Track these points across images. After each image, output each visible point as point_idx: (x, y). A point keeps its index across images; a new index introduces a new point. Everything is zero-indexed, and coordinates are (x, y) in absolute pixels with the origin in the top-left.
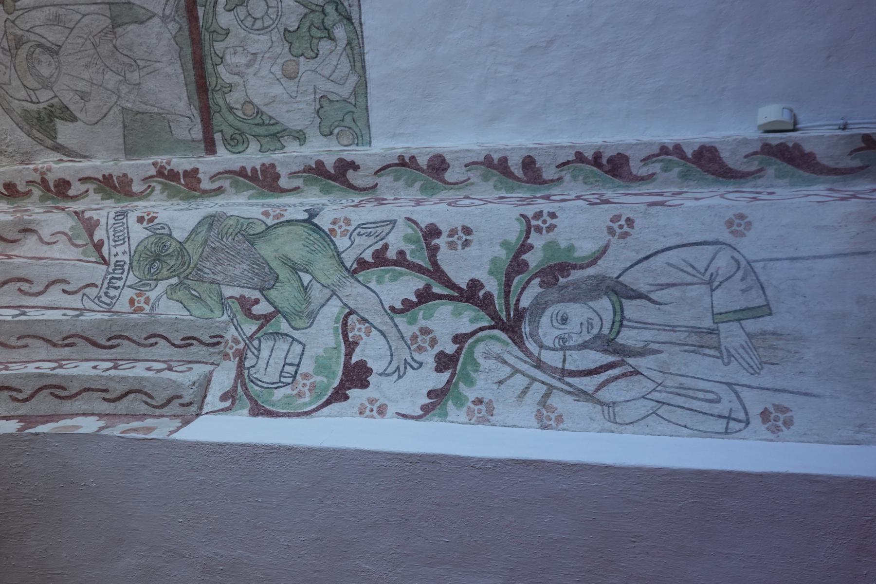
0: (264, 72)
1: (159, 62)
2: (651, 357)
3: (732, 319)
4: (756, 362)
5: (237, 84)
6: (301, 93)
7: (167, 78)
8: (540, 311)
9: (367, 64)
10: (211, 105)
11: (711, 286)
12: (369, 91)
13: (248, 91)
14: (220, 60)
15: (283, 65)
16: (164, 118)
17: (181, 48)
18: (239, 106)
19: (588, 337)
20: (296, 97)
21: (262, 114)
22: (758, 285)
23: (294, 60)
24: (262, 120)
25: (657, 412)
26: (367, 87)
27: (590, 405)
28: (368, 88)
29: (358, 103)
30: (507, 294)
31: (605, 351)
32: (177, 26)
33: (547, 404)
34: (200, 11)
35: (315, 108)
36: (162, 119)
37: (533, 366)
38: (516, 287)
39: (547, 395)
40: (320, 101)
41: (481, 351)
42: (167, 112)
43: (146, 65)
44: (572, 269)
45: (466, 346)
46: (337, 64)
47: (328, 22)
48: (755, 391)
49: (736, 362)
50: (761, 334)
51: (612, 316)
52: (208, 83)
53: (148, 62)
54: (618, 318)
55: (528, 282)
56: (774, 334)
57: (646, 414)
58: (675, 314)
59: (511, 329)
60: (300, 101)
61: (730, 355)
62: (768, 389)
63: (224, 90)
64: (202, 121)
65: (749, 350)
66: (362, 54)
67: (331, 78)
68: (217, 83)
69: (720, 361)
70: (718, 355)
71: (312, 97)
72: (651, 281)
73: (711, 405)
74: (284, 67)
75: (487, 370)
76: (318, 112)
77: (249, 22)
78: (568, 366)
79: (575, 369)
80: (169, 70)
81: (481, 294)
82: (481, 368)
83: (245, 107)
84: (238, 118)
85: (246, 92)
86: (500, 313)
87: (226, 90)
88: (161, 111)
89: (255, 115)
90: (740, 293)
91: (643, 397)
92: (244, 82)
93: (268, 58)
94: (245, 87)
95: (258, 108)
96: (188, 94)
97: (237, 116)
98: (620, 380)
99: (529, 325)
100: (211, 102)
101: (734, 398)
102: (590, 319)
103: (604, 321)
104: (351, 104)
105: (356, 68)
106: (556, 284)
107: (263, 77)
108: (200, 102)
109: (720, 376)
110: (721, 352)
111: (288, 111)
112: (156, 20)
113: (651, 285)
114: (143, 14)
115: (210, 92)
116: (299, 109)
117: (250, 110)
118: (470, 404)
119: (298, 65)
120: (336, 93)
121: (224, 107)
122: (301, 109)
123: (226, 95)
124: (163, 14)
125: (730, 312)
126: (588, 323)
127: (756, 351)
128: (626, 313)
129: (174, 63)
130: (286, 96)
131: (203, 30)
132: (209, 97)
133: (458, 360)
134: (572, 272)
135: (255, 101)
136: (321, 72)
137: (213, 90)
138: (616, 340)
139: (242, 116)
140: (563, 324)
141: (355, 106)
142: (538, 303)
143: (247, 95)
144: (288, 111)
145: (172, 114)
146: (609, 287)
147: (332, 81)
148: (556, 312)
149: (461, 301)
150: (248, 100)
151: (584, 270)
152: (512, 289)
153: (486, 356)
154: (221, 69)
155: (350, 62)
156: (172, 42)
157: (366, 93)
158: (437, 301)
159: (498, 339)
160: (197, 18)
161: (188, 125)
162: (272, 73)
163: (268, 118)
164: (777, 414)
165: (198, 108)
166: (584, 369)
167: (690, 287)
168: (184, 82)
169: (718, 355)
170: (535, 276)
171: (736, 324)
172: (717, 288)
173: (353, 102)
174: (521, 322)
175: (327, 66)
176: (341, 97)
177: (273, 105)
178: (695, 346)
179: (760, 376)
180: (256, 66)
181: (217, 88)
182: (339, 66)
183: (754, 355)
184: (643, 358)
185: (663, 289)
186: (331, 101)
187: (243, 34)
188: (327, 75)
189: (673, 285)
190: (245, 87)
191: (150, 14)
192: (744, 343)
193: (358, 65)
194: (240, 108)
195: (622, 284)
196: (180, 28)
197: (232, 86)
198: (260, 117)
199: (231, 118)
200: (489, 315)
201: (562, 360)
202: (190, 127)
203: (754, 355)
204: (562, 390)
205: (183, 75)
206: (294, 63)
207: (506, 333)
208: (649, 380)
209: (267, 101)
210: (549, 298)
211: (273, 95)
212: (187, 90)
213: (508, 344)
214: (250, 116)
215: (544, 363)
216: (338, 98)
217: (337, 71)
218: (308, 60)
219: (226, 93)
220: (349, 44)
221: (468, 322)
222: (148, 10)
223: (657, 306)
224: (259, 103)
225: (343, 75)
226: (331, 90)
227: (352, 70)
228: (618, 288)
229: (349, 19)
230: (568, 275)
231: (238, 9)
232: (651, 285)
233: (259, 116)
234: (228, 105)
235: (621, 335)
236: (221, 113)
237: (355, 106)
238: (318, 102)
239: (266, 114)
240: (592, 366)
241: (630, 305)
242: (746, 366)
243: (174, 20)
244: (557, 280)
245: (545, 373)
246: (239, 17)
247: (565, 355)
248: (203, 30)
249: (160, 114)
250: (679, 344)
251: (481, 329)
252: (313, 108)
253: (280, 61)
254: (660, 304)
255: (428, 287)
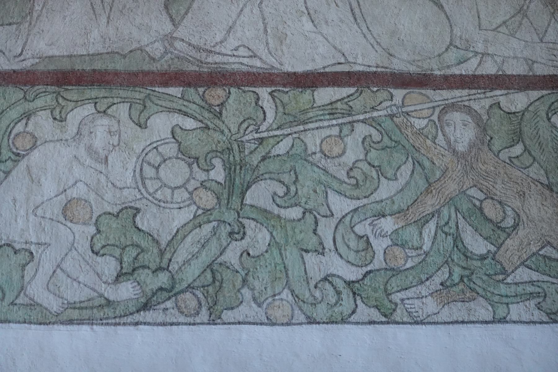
0: (77, 171)
1: (108, 22)
5: (64, 130)
6: (40, 224)
7: (83, 31)
9: (75, 327)
10: (36, 88)
12: (33, 326)
13: (52, 144)
14: (102, 110)
15: (86, 201)
16: (23, 18)
17: (125, 56)
18: (30, 128)
20: (36, 215)
21: (15, 161)
23: (91, 218)
24: (6, 161)
26: (40, 324)
28: (38, 326)
29: (16, 308)
32: (158, 55)
34: (175, 91)
35: (15, 242)
36: (24, 14)
40: (26, 250)
42: (33, 23)
43: (106, 4)
46: (79, 282)
47: (144, 275)
52: (70, 88)
53: (109, 8)
60: (28, 221)
63: (58, 110)
64: (14, 71)
66: (91, 322)
67: (59, 271)
68: (68, 100)
71: (34, 240)
74: (83, 202)
76: (9, 245)
77: (156, 159)
80: (95, 34)
83: (29, 137)
84: (12, 125)
85: (51, 141)
87: (57, 113)
88: (35, 15)
89: (15, 150)
92: (67, 140)
93: (99, 180)
94: (58, 141)
95: (24, 156)
96: (56, 56)
97: (16, 123)
100: (41, 88)
104: (17, 298)
105: (70, 311)
107: (70, 170)
108: (43, 73)
111: (15, 200)
112: (168, 27)
114: (178, 11)
115: (57, 89)
116: (16, 216)
117: (23, 144)
119: (84, 224)
120: (35, 275)
121: (32, 106)
122: (16, 221)
123: (48, 112)
124: (176, 38)
129: (104, 42)
130: (39, 199)
131: (148, 92)
132: (49, 87)
135: (35, 155)
136: (69, 257)
137: (59, 93)
139: (15, 132)
141: (13, 304)
143: (46, 142)
144: (15, 200)
145: (29, 31)
147: (54, 272)
150: (38, 143)
154: (89, 109)
155: (81, 302)
156: (135, 46)
157: (30, 323)
160: (165, 84)
161: (10, 51)
162: (76, 182)
163: (8, 169)
165: (34, 68)
168: (75, 53)
173: (17, 301)
175: (77, 266)
176: (29, 283)
177: (27, 178)
180: (88, 161)
181: (60, 100)
182: (75, 284)
186: (24, 267)
187: (138, 147)
188: (64, 266)
190: (58, 141)
191: (177, 20)
193: (75, 314)
194: (27, 129)
196: (154, 59)
197: (61, 121)
198: (10, 157)
199: (14, 114)
202: (6, 53)
205: (85, 53)
206: (87, 217)
209: (34, 170)
211: (43, 180)
212: (63, 57)
214: (13, 143)
216: (27, 279)
217: (69, 280)
218: (89, 238)
219: (52, 112)
220: (109, 303)
222: (183, 18)
224: (32, 158)
225: (61, 289)
226: (41, 269)
227: (69, 303)
229: (146, 307)
231: (174, 145)
233: (13, 157)
234: (34, 113)
236: (23, 100)
237: (13, 304)
238: (24, 246)
239: (14, 167)
243: (166, 52)
246: (162, 144)
248: (148, 92)
249: (31, 13)
252: (16, 239)
253: (92, 197)
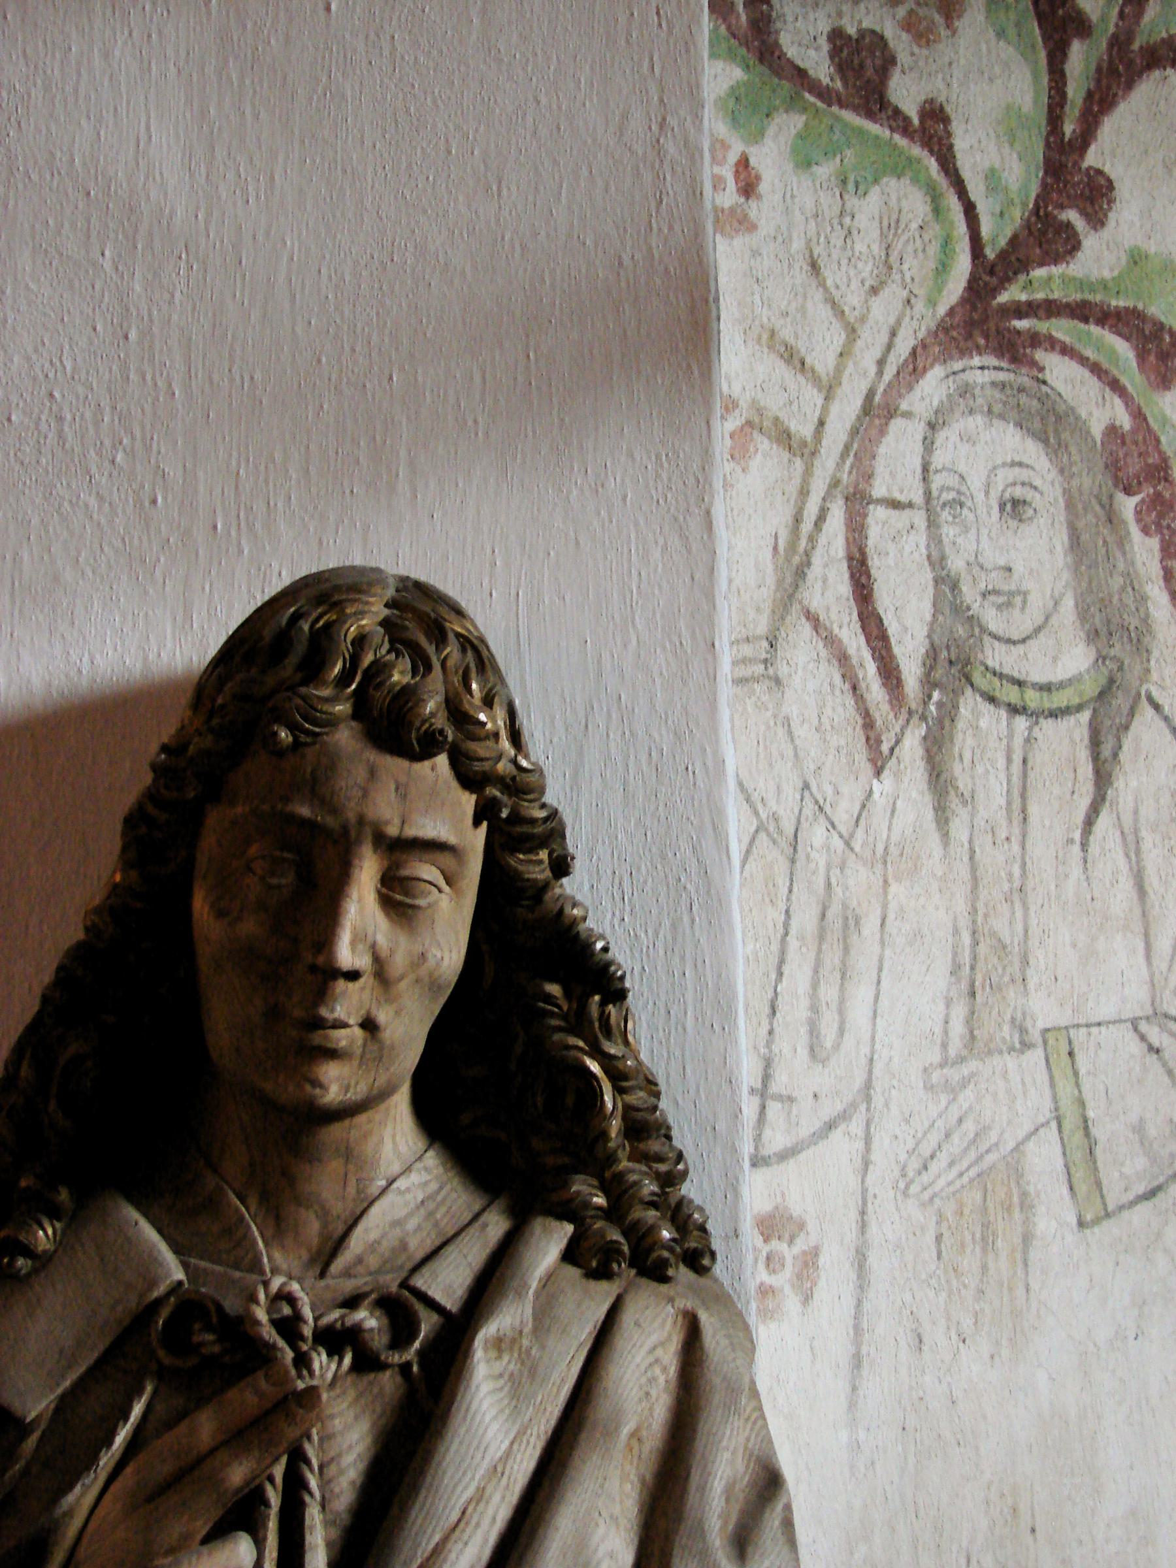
2: (929, 814)
3: (1060, 1093)
4: (941, 1183)
8: (1037, 425)
11: (1148, 1018)
19: (969, 594)
22: (1161, 1179)
25: (762, 836)
27: (767, 594)
30: (1082, 312)
31: (932, 654)
33: (756, 434)
37: (870, 395)
38: (1099, 347)
39: (784, 437)
41: (905, 204)
44: (1162, 541)
45: (917, 151)
48: (853, 1182)
49: (934, 1111)
50: (1024, 1195)
51: (1037, 677)
54: (1032, 698)
55: (1116, 386)
56: (1027, 1239)
57: (755, 797)
58: (1058, 897)
59: (976, 316)
61: (953, 1090)
62: (863, 1226)
65: (972, 1155)
69: (936, 1058)
70: (952, 1052)
72: (1147, 812)
73: (803, 1030)
75: (847, 220)
78: (877, 515)
79: (871, 543)
81: (1072, 216)
82: (852, 202)
86: (1022, 278)
90: (1133, 1118)
91: (806, 786)
98: (850, 701)
99: (993, 384)
101: (830, 1109)
102: (1024, 602)
103: (1020, 649)
106: (1116, 485)
109: (890, 1059)
110: (961, 1060)
113: (1136, 812)
118: (737, 148)
125: (1077, 1085)
126: (1011, 594)
127: (971, 1181)
128: (1047, 724)
133: (870, 115)
134: (1154, 543)
138: (969, 691)
140: (1002, 507)
142: (1059, 418)
146: (1120, 668)
148: (1037, 482)
149: (1048, 144)
151: (1162, 583)
152: (1095, 330)
153: (891, 226)
158: (1043, 54)
159: (943, 268)
164: (789, 1262)
166: (873, 572)
167: (1141, 946)
169: (952, 1052)
170: (1138, 415)
171: (1046, 1113)
172: (1143, 1038)
174: (1000, 354)
178: (973, 968)
179: (899, 1197)
183: (961, 1175)
184: (924, 786)
185: (1127, 855)
189: (1141, 891)
192: (993, 1137)
195: (1132, 713)
200: (1014, 241)
201: (897, 496)
203: (961, 1175)
204: (804, 493)
207: (963, 301)
208: (857, 807)
210: (1076, 457)
213: (932, 303)
215: (882, 432)
221: (987, 165)
223: (1077, 835)
228: (1120, 701)
230: (1146, 531)
232: (1136, 812)
235: (985, 707)
240: (884, 602)
241: (1072, 740)
242: (926, 1149)
244: (1128, 491)
245: (854, 432)
247: (910, 505)
250: (974, 911)
251: (970, 210)
254: (1084, 846)
255: (1082, 26)
